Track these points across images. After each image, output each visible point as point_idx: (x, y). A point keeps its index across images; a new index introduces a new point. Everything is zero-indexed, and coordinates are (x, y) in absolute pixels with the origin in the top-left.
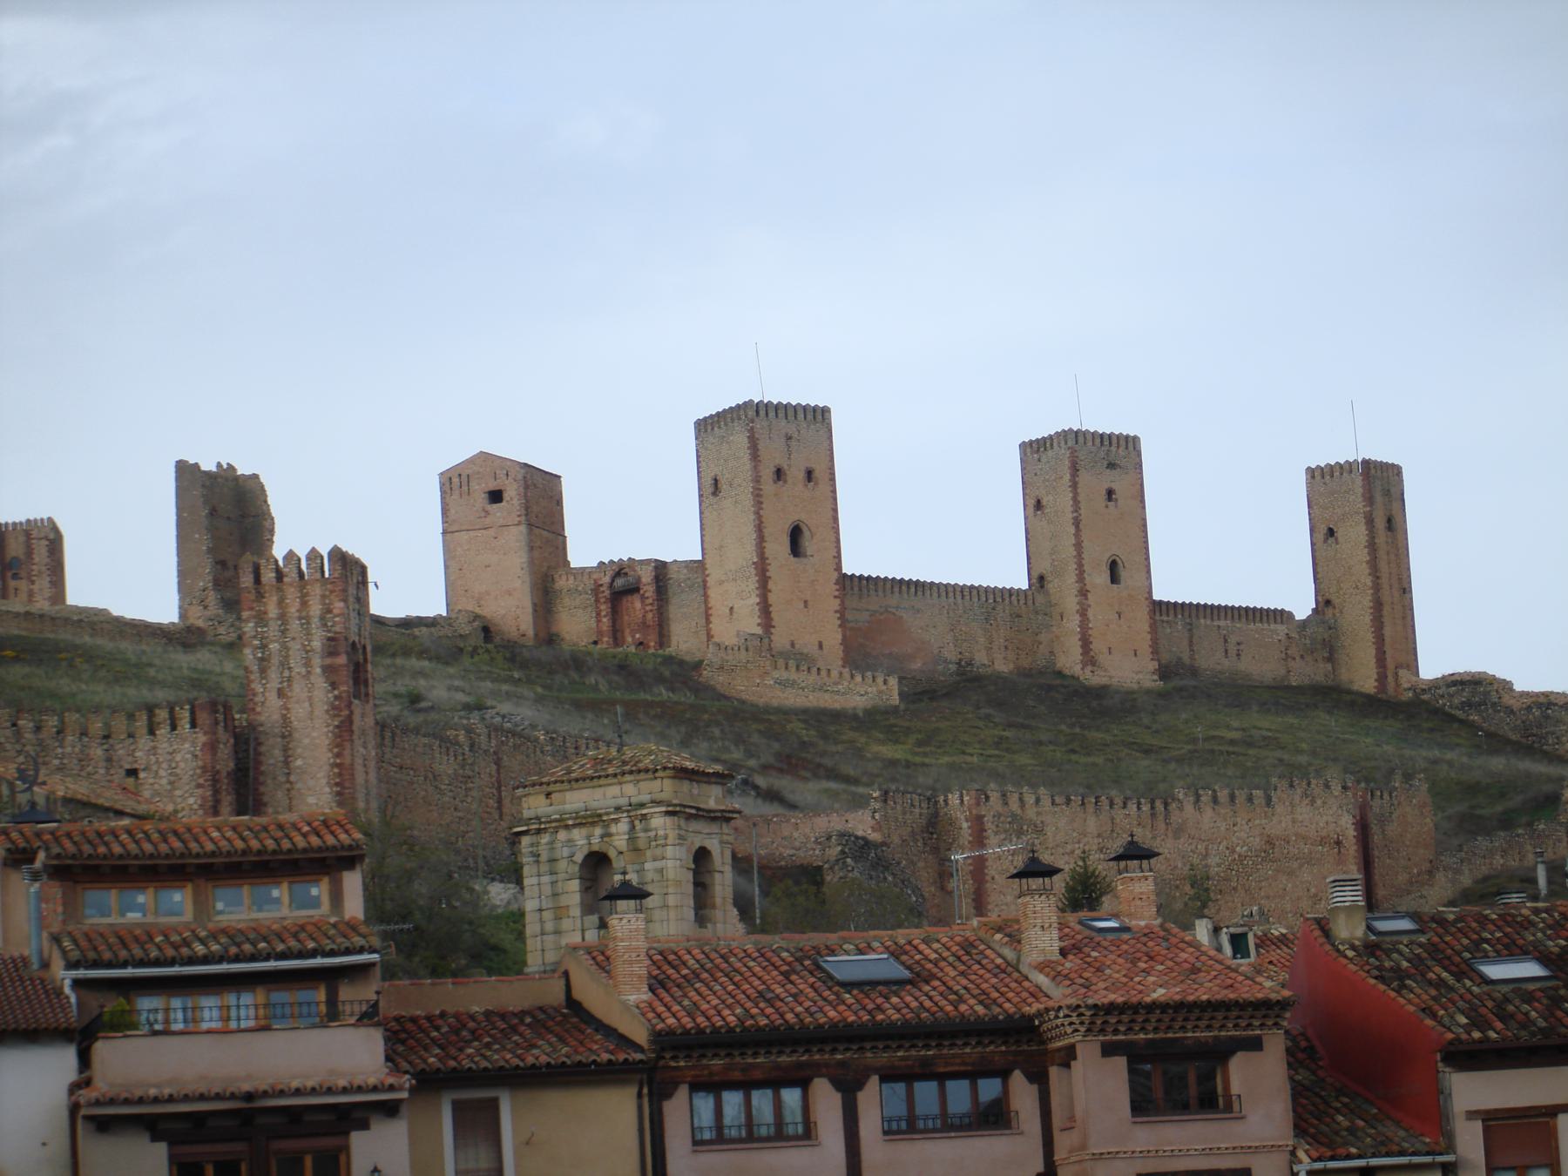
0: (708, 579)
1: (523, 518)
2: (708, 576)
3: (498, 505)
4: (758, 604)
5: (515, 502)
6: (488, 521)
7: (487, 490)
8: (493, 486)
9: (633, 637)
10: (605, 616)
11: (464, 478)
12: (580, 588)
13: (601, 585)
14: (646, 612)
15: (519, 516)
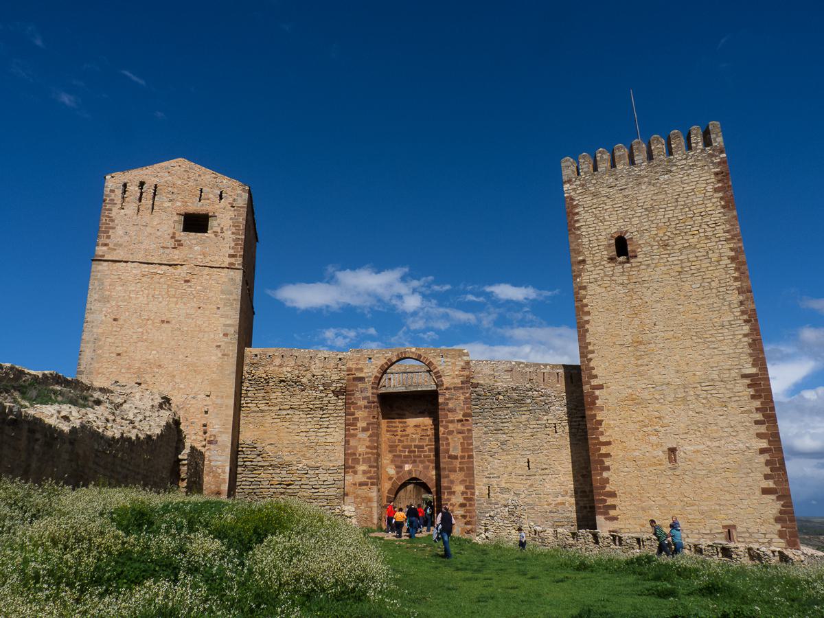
0: (597, 392)
1: (240, 260)
2: (600, 387)
3: (199, 234)
4: (762, 451)
5: (228, 234)
6: (176, 256)
7: (182, 212)
8: (195, 207)
9: (399, 468)
10: (364, 430)
11: (148, 188)
12: (304, 380)
13: (362, 379)
14: (451, 432)
15: (231, 256)
